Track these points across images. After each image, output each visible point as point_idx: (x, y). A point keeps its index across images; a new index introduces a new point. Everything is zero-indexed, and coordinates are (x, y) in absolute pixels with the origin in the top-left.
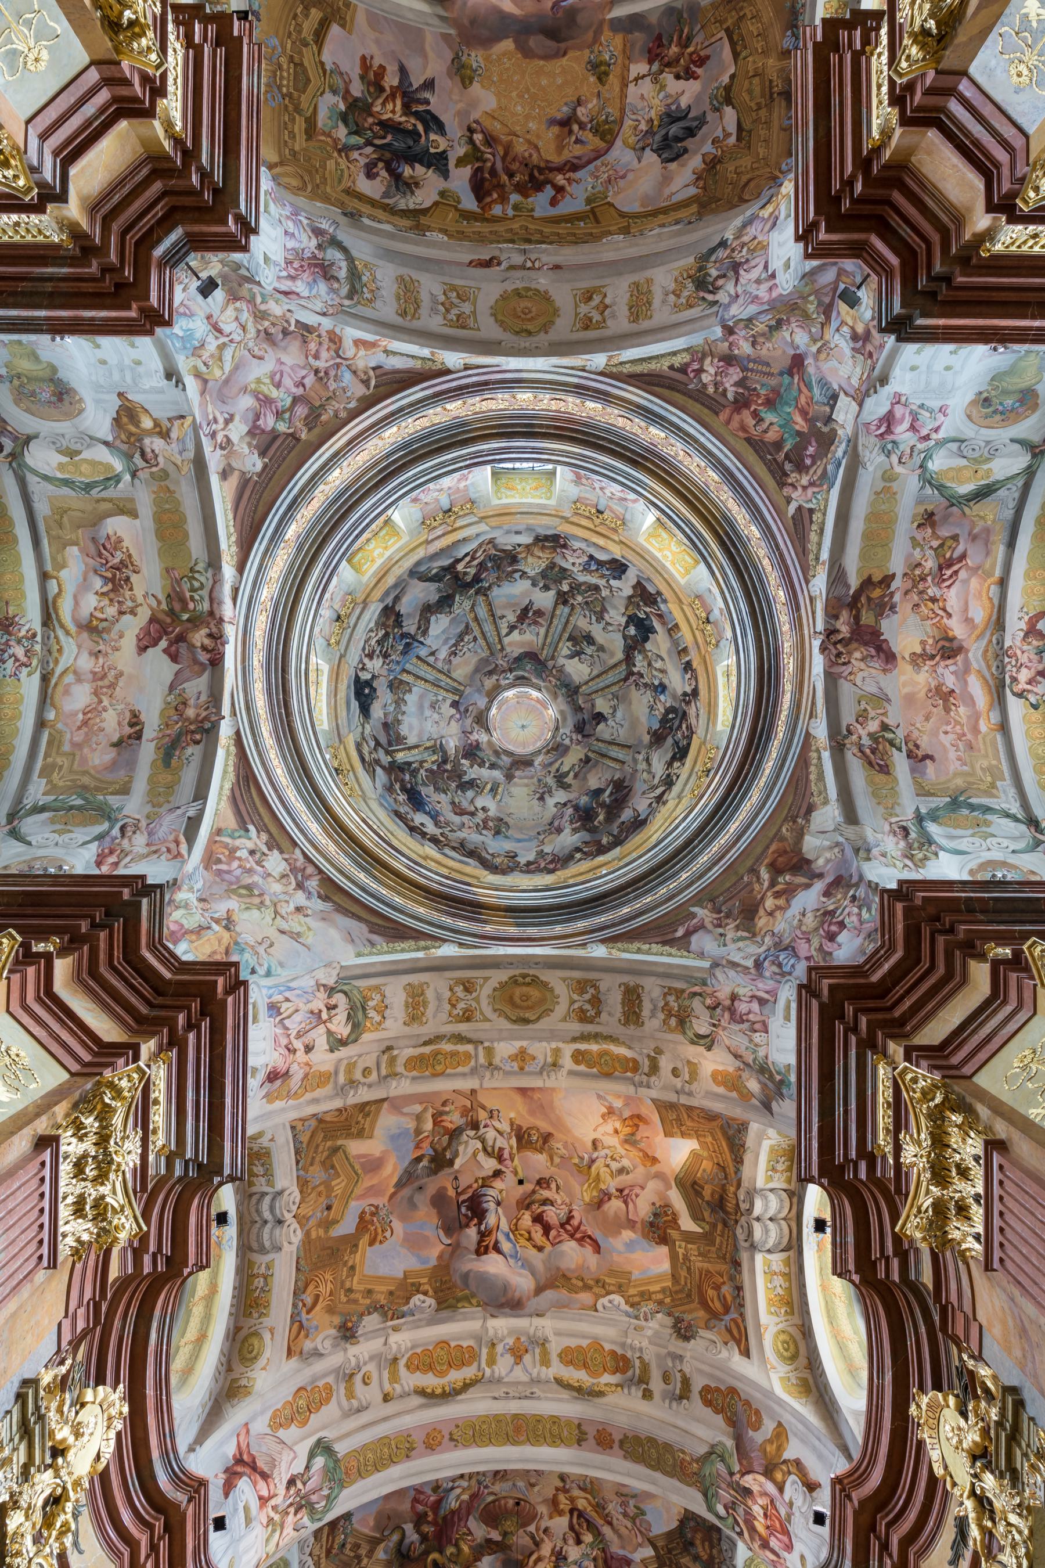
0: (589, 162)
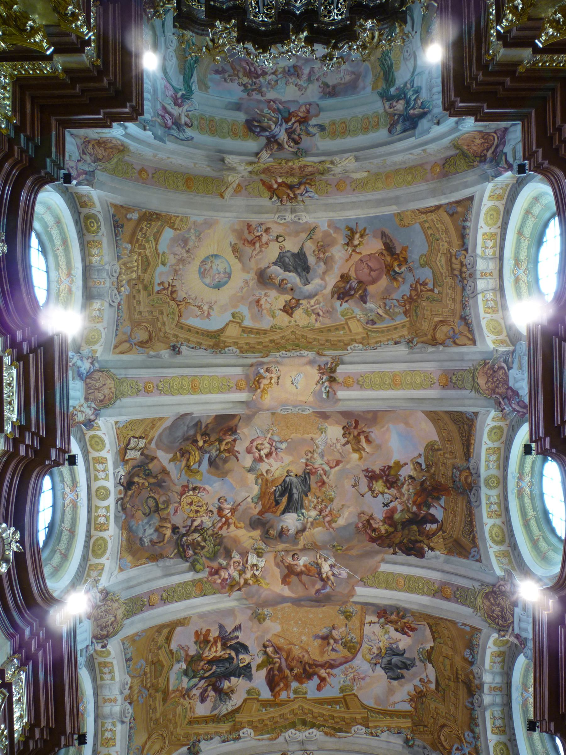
0: (341, 664)
